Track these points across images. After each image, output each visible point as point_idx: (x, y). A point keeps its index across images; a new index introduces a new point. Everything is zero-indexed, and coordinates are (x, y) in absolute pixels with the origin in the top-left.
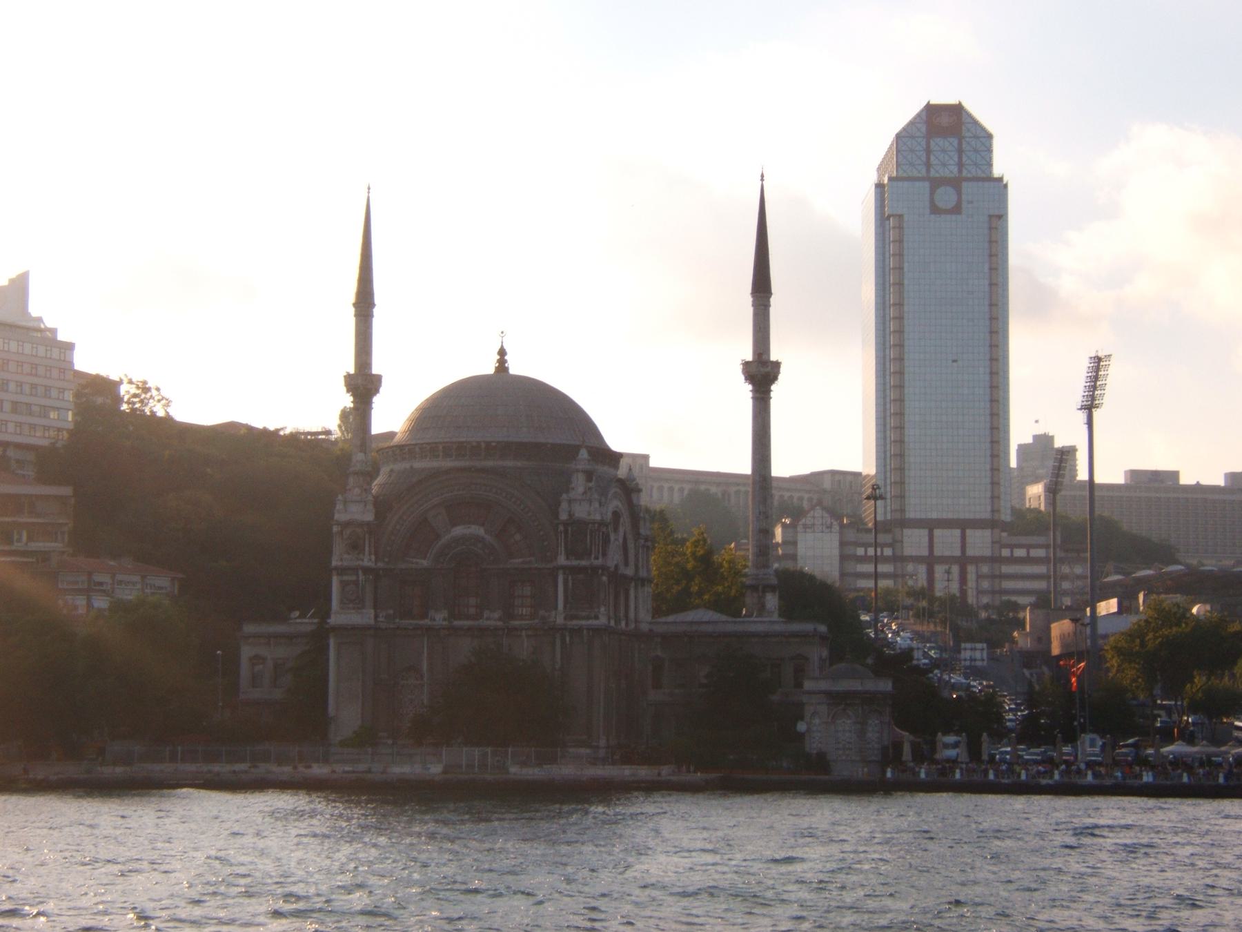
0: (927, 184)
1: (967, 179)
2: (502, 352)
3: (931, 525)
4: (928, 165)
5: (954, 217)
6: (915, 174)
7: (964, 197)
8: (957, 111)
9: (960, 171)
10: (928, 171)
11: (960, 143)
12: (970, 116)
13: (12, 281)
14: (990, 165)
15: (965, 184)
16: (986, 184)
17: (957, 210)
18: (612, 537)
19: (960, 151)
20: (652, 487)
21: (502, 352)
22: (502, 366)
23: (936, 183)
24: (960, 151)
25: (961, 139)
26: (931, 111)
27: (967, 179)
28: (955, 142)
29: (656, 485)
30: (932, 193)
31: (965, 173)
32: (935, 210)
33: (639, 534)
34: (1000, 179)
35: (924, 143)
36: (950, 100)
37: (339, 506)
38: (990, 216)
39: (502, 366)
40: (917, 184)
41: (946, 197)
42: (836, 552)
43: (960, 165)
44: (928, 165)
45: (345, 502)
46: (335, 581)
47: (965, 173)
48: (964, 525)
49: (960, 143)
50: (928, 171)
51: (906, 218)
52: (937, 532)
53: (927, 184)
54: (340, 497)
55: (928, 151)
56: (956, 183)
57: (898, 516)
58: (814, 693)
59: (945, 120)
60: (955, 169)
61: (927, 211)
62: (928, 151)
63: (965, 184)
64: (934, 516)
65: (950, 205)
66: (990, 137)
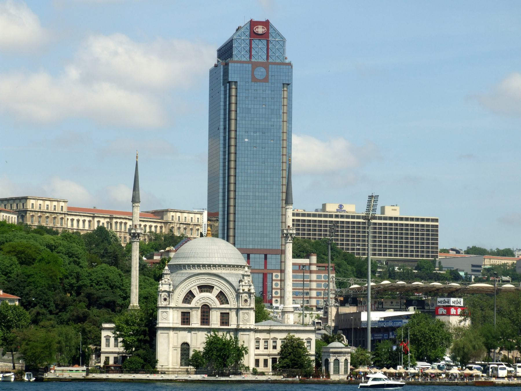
7: (270, 73)
8: (266, 24)
16: (282, 67)
17: (266, 80)
23: (255, 65)
25: (268, 42)
26: (253, 24)
27: (273, 64)
29: (70, 218)
32: (254, 80)
34: (290, 64)
38: (283, 84)
40: (245, 65)
41: (260, 73)
47: (270, 60)
50: (250, 57)
51: (238, 84)
53: (250, 65)
55: (251, 48)
56: (266, 65)
59: (260, 30)
60: (265, 57)
61: (250, 80)
62: (251, 48)
63: (270, 66)
64: (251, 247)
65: (262, 78)
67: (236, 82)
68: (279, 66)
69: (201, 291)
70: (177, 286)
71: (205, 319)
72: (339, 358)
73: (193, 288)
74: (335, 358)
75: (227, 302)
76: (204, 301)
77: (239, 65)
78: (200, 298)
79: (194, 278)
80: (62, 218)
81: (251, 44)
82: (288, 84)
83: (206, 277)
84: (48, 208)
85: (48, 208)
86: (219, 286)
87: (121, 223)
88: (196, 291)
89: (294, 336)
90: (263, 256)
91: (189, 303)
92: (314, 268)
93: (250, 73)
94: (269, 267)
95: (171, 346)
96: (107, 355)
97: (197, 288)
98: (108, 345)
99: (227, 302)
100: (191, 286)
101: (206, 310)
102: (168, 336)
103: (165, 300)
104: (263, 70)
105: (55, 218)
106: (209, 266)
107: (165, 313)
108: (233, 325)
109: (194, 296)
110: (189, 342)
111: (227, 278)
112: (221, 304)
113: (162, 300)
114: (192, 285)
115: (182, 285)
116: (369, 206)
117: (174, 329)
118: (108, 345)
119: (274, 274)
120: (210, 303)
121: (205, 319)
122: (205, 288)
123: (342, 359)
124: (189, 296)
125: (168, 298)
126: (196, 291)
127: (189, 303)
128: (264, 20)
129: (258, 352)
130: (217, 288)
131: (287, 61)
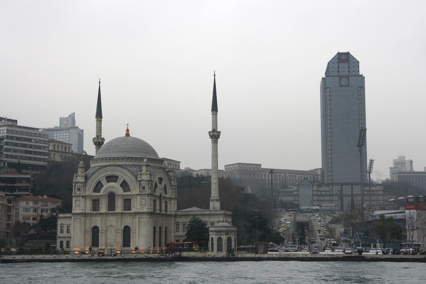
0: (338, 78)
1: (351, 76)
2: (128, 130)
3: (341, 185)
4: (339, 72)
5: (347, 88)
6: (334, 74)
8: (348, 54)
9: (349, 73)
10: (339, 74)
11: (349, 65)
12: (352, 56)
13: (70, 116)
14: (359, 71)
15: (350, 77)
16: (357, 77)
17: (348, 85)
18: (159, 185)
19: (349, 67)
20: (262, 174)
21: (128, 130)
22: (128, 135)
23: (341, 77)
24: (349, 67)
26: (339, 54)
27: (351, 76)
28: (347, 64)
30: (340, 80)
31: (350, 74)
32: (341, 86)
33: (171, 185)
34: (362, 75)
35: (337, 65)
36: (346, 51)
37: (75, 178)
39: (128, 135)
40: (335, 78)
41: (344, 81)
42: (311, 194)
43: (349, 71)
44: (339, 72)
45: (76, 177)
46: (74, 199)
47: (350, 74)
48: (352, 185)
49: (349, 65)
50: (339, 74)
51: (332, 88)
52: (343, 187)
53: (338, 78)
54: (75, 175)
55: (339, 67)
56: (347, 77)
57: (331, 182)
58: (213, 231)
59: (344, 57)
61: (338, 86)
62: (339, 67)
63: (350, 77)
64: (342, 181)
65: (346, 84)
66: (358, 62)
67: (330, 88)
68: (355, 77)
69: (108, 182)
70: (89, 178)
71: (111, 206)
72: (222, 237)
73: (102, 179)
74: (218, 236)
75: (129, 190)
76: (110, 190)
77: (331, 78)
78: (107, 186)
79: (102, 170)
80: (258, 174)
81: (338, 65)
82: (362, 87)
83: (112, 168)
84: (250, 169)
85: (250, 169)
86: (124, 175)
87: (293, 176)
88: (104, 182)
89: (198, 218)
90: (350, 187)
91: (99, 192)
92: (381, 193)
93: (338, 82)
94: (354, 193)
95: (83, 229)
96: (61, 240)
97: (105, 179)
98: (62, 232)
99: (129, 190)
100: (100, 177)
101: (111, 197)
102: (81, 220)
103: (79, 189)
104: (346, 79)
105: (254, 174)
106: (114, 159)
107: (78, 201)
108: (133, 210)
109: (102, 186)
110: (99, 226)
111: (129, 169)
112: (124, 192)
113: (76, 190)
114: (101, 176)
115: (93, 177)
116: (360, 136)
117: (85, 215)
118: (62, 232)
119: (358, 197)
120: (115, 191)
121: (111, 206)
122: (111, 178)
123: (224, 238)
124: (98, 187)
125: (81, 188)
126: (104, 182)
127: (99, 192)
128: (347, 52)
129: (177, 234)
130: (121, 178)
131: (360, 73)
